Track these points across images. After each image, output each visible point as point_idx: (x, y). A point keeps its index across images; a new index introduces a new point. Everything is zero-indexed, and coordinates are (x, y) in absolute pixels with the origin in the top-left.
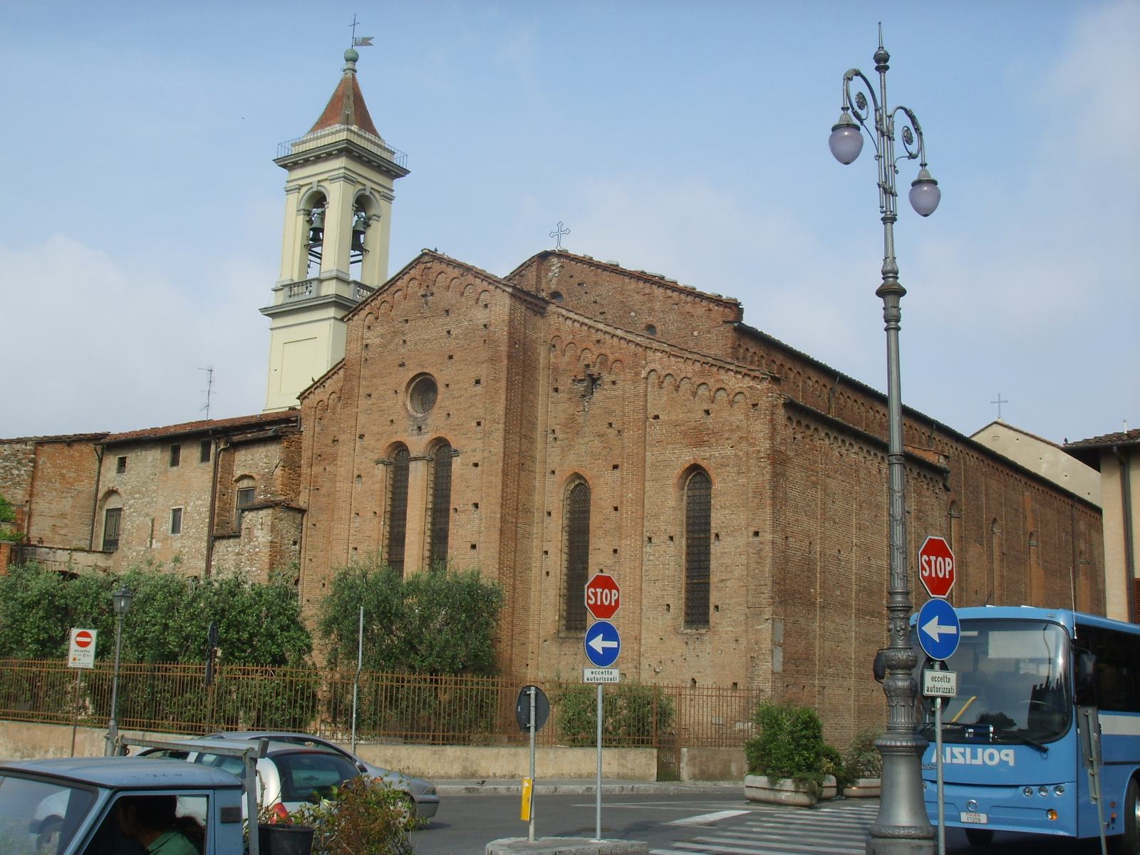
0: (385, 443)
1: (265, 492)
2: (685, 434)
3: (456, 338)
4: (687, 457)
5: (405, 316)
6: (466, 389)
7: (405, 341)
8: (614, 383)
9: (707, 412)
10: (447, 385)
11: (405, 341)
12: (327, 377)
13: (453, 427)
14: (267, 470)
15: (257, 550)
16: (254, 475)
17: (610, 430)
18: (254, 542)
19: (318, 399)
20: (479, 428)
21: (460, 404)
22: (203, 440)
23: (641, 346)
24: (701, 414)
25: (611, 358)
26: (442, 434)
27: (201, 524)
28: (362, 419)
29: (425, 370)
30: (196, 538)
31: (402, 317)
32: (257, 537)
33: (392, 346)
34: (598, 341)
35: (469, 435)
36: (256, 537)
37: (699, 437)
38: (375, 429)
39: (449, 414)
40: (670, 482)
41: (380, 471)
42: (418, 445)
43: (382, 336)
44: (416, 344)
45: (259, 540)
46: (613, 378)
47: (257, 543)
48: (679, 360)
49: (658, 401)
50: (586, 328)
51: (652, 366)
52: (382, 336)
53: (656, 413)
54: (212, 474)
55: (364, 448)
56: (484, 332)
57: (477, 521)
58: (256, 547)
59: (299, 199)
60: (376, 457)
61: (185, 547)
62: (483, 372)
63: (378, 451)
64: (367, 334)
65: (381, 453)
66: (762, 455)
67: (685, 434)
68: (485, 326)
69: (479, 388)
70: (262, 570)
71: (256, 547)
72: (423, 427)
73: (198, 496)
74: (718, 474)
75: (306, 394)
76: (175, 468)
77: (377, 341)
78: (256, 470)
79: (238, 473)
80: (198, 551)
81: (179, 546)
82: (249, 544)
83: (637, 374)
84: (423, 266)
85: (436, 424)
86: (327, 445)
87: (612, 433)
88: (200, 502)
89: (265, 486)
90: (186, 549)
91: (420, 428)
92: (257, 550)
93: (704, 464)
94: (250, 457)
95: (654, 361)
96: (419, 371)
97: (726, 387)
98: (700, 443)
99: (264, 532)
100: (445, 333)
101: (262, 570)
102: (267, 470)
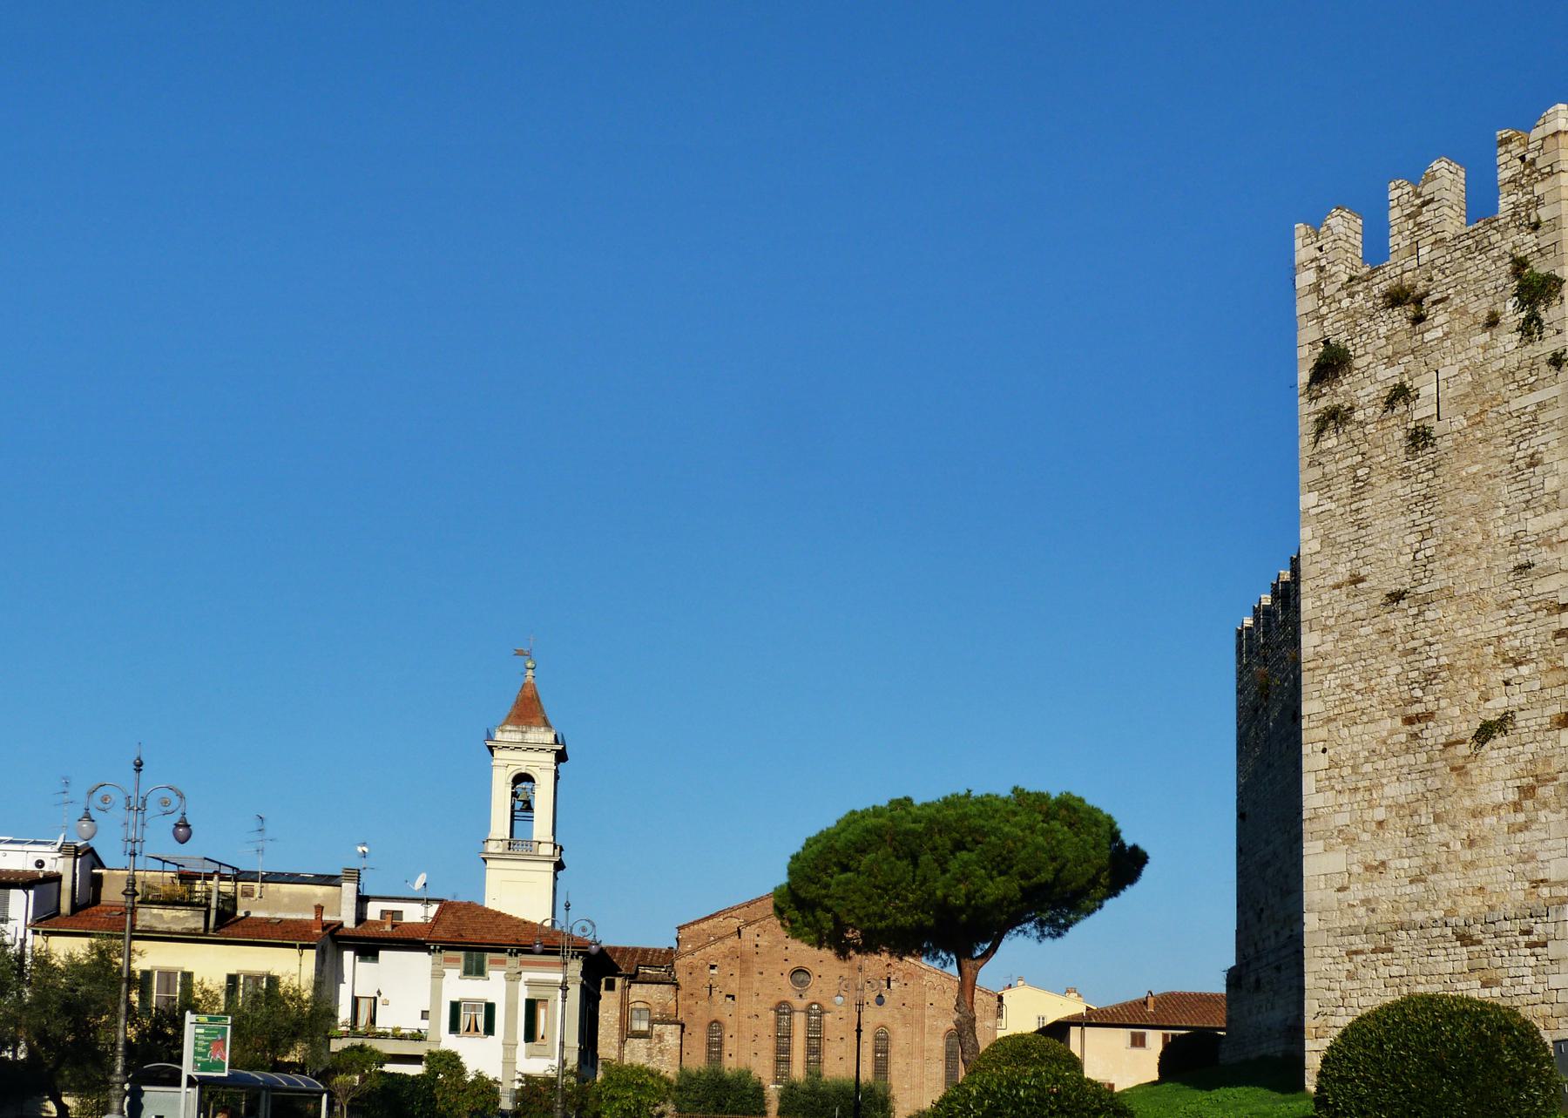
0: (773, 1002)
1: (661, 1014)
7: (787, 948)
8: (906, 984)
10: (820, 976)
11: (787, 948)
33: (778, 949)
42: (799, 1004)
57: (844, 1047)
59: (508, 774)
70: (673, 1059)
77: (766, 944)
85: (812, 994)
88: (607, 1015)
91: (801, 996)
101: (673, 1059)
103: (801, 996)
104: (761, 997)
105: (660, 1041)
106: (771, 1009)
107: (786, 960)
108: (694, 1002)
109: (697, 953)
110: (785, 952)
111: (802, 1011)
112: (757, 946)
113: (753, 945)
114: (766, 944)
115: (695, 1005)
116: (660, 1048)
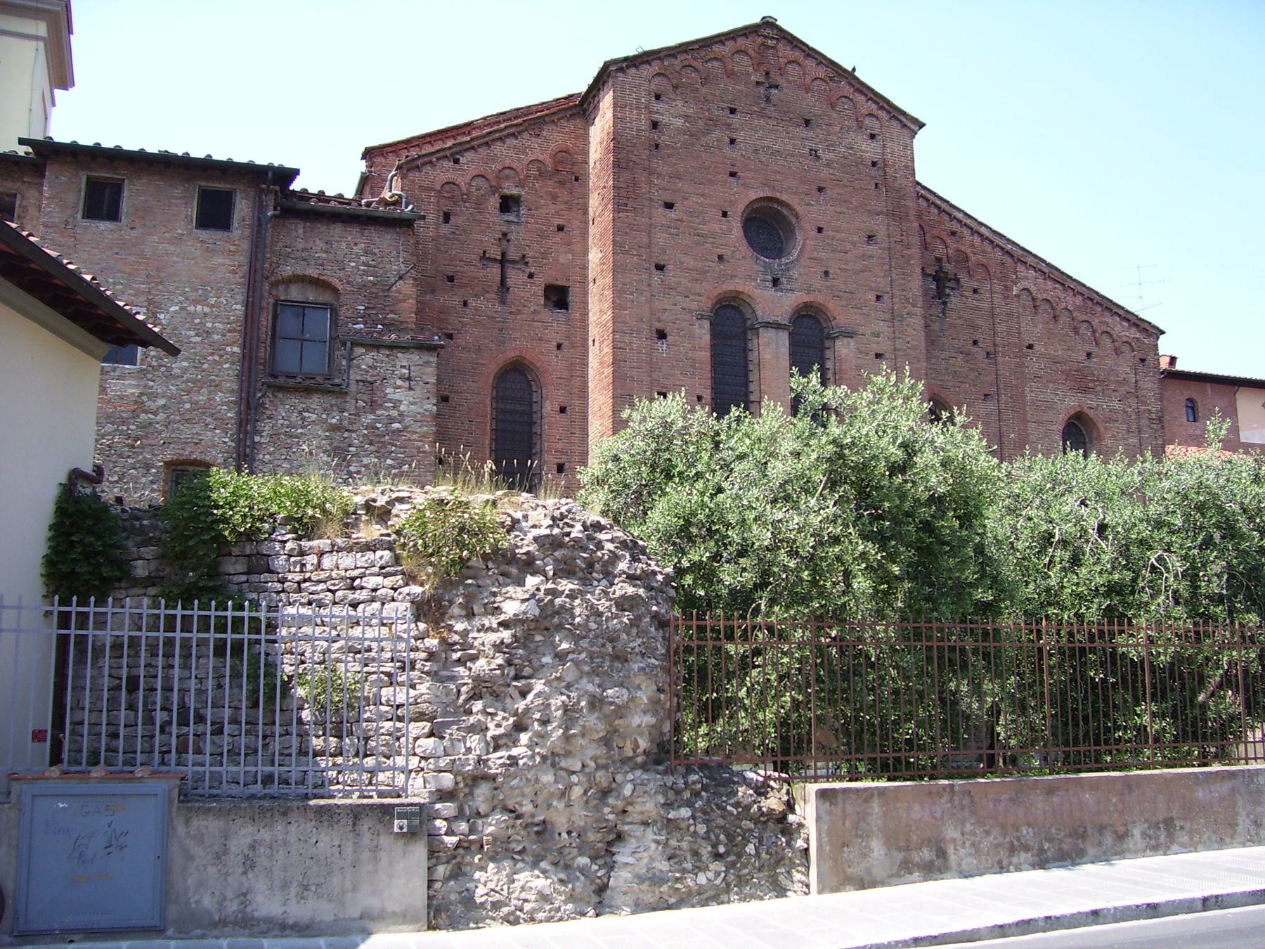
1: (366, 318)
2: (1067, 374)
3: (827, 165)
4: (1072, 402)
5: (732, 102)
6: (854, 244)
7: (732, 141)
9: (1089, 355)
10: (820, 230)
11: (732, 141)
12: (468, 146)
13: (837, 293)
14: (372, 278)
15: (396, 426)
16: (335, 282)
17: (976, 349)
18: (388, 409)
19: (443, 177)
20: (879, 305)
21: (847, 262)
22: (204, 184)
23: (1012, 256)
24: (1083, 357)
25: (973, 258)
26: (818, 298)
27: (212, 354)
28: (661, 238)
29: (778, 195)
30: (195, 381)
31: (723, 101)
32: (397, 404)
33: (710, 139)
34: (953, 233)
35: (865, 310)
36: (390, 400)
37: (1083, 382)
38: (690, 262)
39: (826, 273)
40: (1054, 428)
41: (703, 332)
43: (686, 117)
44: (756, 151)
45: (402, 408)
46: (975, 284)
47: (394, 413)
48: (1057, 286)
49: (1033, 328)
50: (936, 211)
51: (1025, 284)
52: (686, 117)
53: (1031, 342)
54: (243, 259)
55: (668, 289)
56: (873, 172)
58: (392, 420)
60: (695, 306)
61: (154, 396)
62: (880, 226)
63: (699, 298)
64: (657, 106)
65: (706, 304)
66: (1154, 416)
67: (1067, 374)
68: (874, 164)
69: (872, 249)
71: (392, 420)
72: (783, 280)
73: (193, 295)
74: (1106, 429)
75: (419, 163)
76: (103, 225)
77: (679, 122)
78: (341, 274)
79: (288, 270)
80: (205, 409)
81: (137, 391)
82: (373, 412)
83: (1007, 288)
84: (760, 40)
86: (468, 263)
87: (979, 353)
89: (366, 308)
90: (161, 402)
91: (775, 282)
92: (396, 426)
93: (1091, 413)
94: (320, 245)
95: (1026, 278)
96: (768, 193)
97: (1112, 332)
98: (1084, 389)
99: (419, 391)
100: (807, 151)
102: (372, 278)
103: (775, 282)
104: (671, 274)
105: (373, 406)
106: (701, 318)
107: (733, 175)
108: (456, 300)
109: (470, 155)
110: (729, 152)
111: (777, 326)
112: (655, 125)
113: (645, 125)
114: (679, 122)
115: (459, 308)
116: (371, 427)
